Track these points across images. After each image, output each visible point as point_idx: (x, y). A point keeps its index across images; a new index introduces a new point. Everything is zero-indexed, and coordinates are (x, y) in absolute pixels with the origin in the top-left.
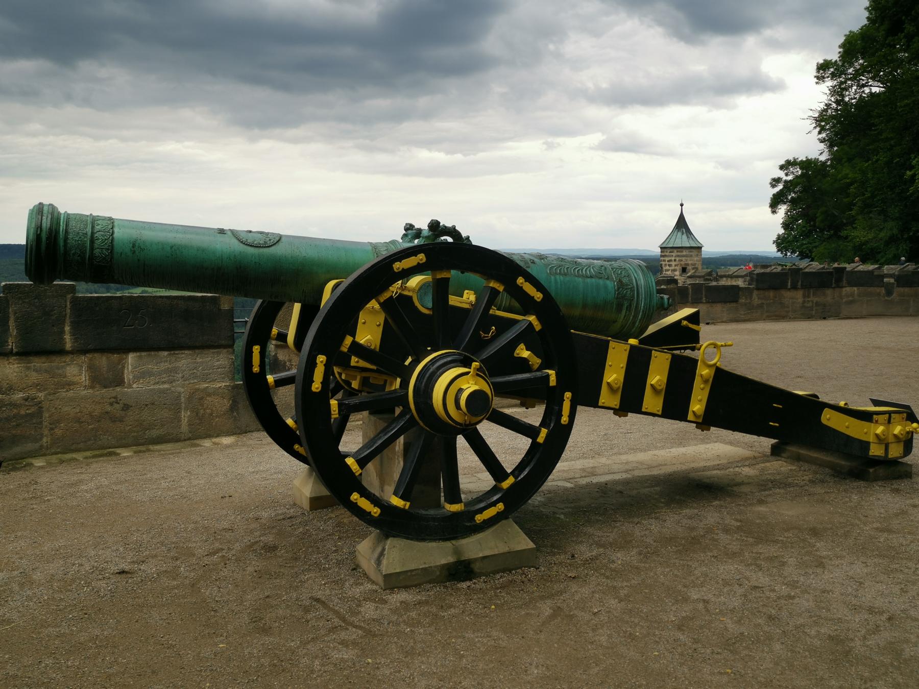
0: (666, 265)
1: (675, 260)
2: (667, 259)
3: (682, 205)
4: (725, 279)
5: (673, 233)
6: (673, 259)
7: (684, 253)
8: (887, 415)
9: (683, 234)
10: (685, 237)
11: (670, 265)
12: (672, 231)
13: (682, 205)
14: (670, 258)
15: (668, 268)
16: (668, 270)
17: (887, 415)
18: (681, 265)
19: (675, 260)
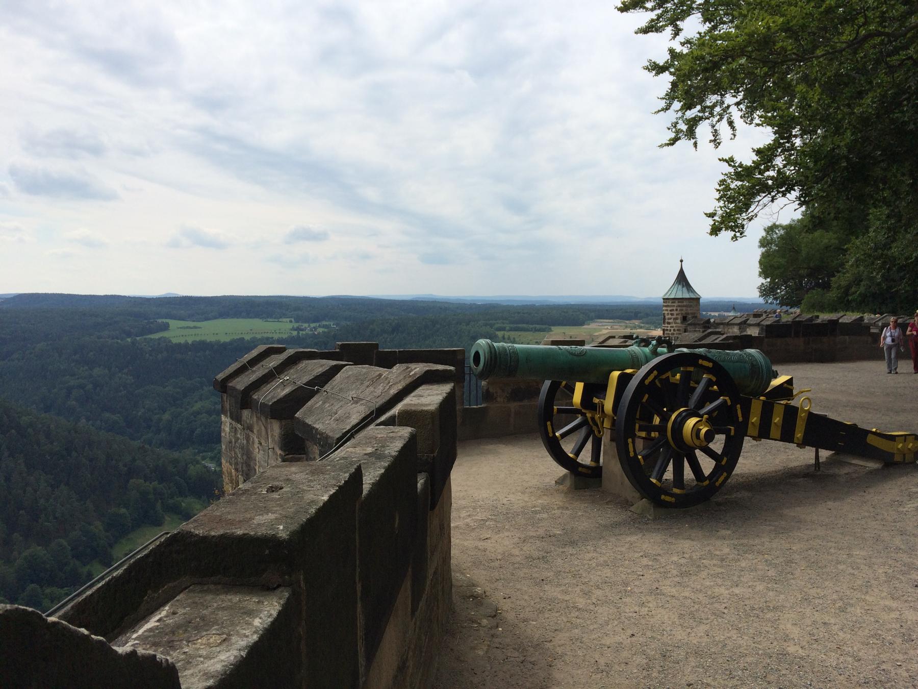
0: (668, 314)
1: (677, 310)
2: (669, 309)
3: (681, 261)
4: (722, 326)
5: (674, 286)
6: (675, 308)
7: (685, 304)
8: (904, 437)
9: (683, 287)
10: (685, 289)
11: (672, 314)
12: (673, 285)
13: (681, 261)
14: (671, 308)
15: (670, 316)
16: (670, 319)
17: (904, 437)
18: (682, 314)
19: (677, 310)
